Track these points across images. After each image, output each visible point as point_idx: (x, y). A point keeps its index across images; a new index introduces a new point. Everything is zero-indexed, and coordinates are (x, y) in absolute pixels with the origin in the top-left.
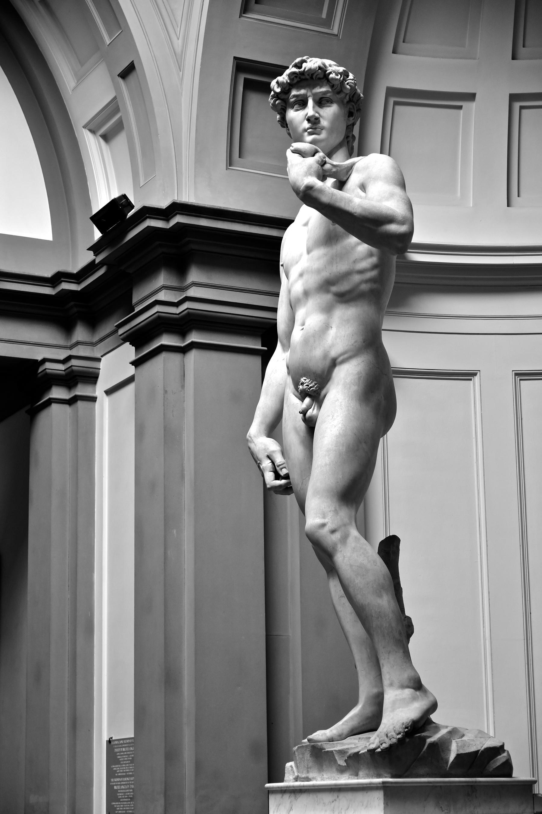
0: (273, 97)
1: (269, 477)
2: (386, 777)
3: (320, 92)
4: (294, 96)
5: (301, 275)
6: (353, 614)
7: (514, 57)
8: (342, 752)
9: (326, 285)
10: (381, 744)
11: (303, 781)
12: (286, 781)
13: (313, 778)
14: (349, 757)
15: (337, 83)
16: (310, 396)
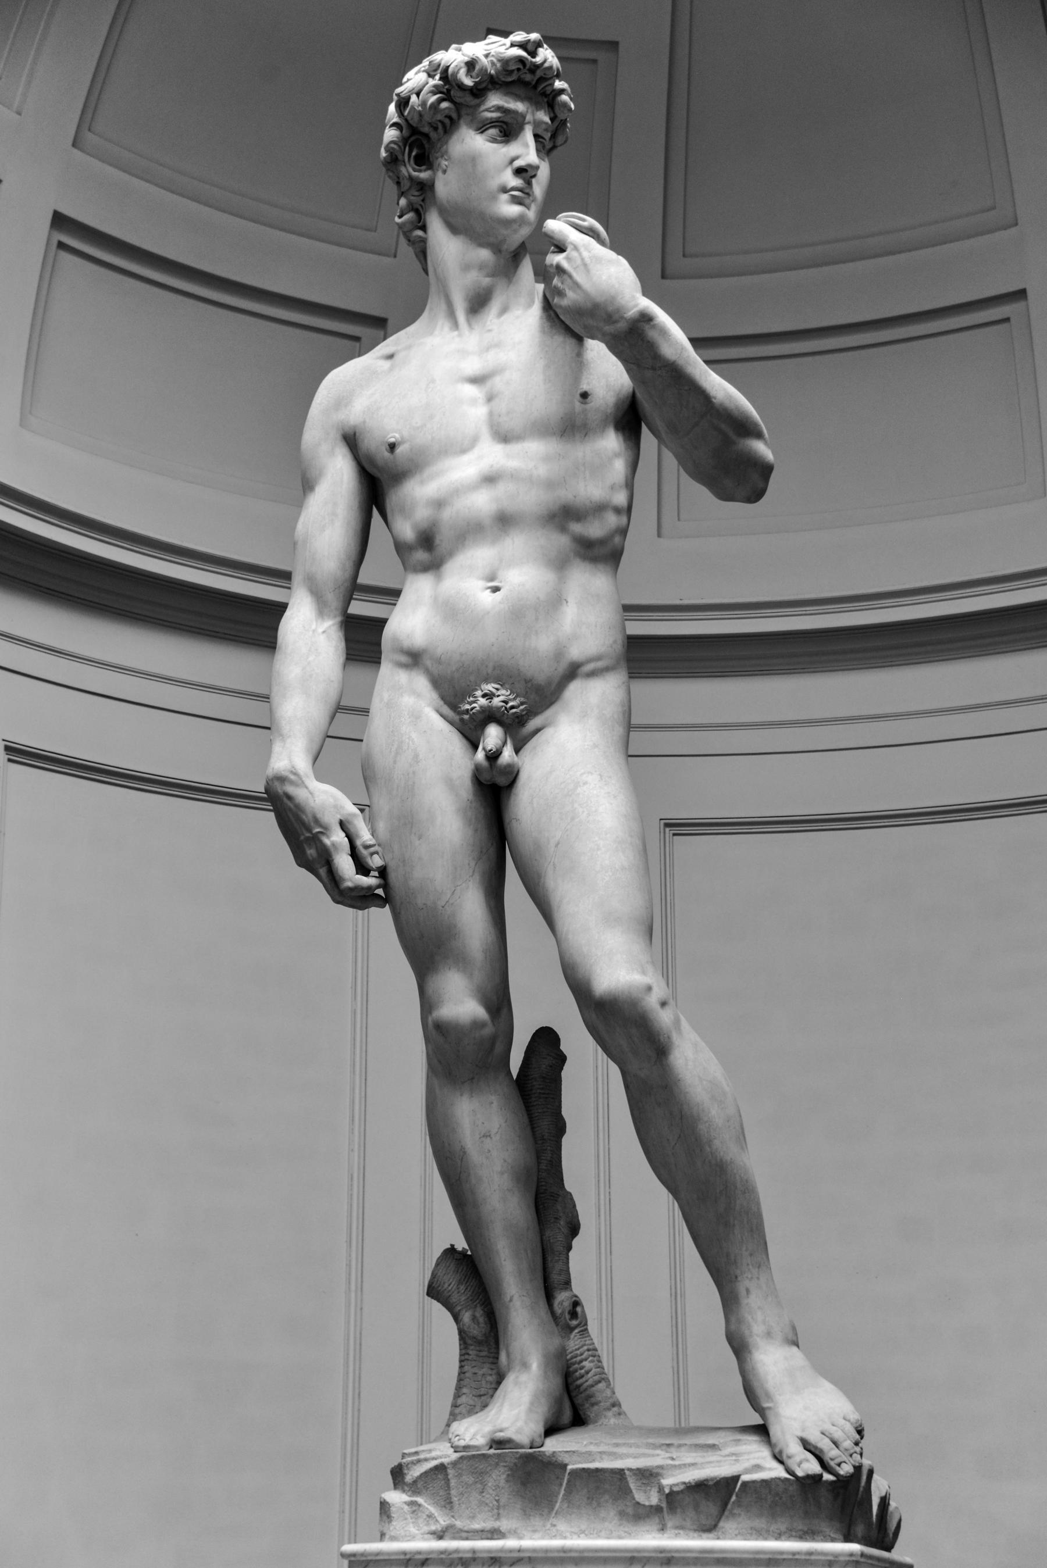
0: (436, 90)
1: (345, 864)
2: (833, 1540)
3: (547, 123)
4: (499, 109)
5: (490, 479)
6: (506, 1176)
7: (76, 143)
8: (648, 1476)
9: (563, 516)
10: (839, 1465)
11: (467, 1539)
12: (394, 1539)
13: (509, 1532)
14: (700, 1487)
15: (561, 116)
16: (500, 722)
